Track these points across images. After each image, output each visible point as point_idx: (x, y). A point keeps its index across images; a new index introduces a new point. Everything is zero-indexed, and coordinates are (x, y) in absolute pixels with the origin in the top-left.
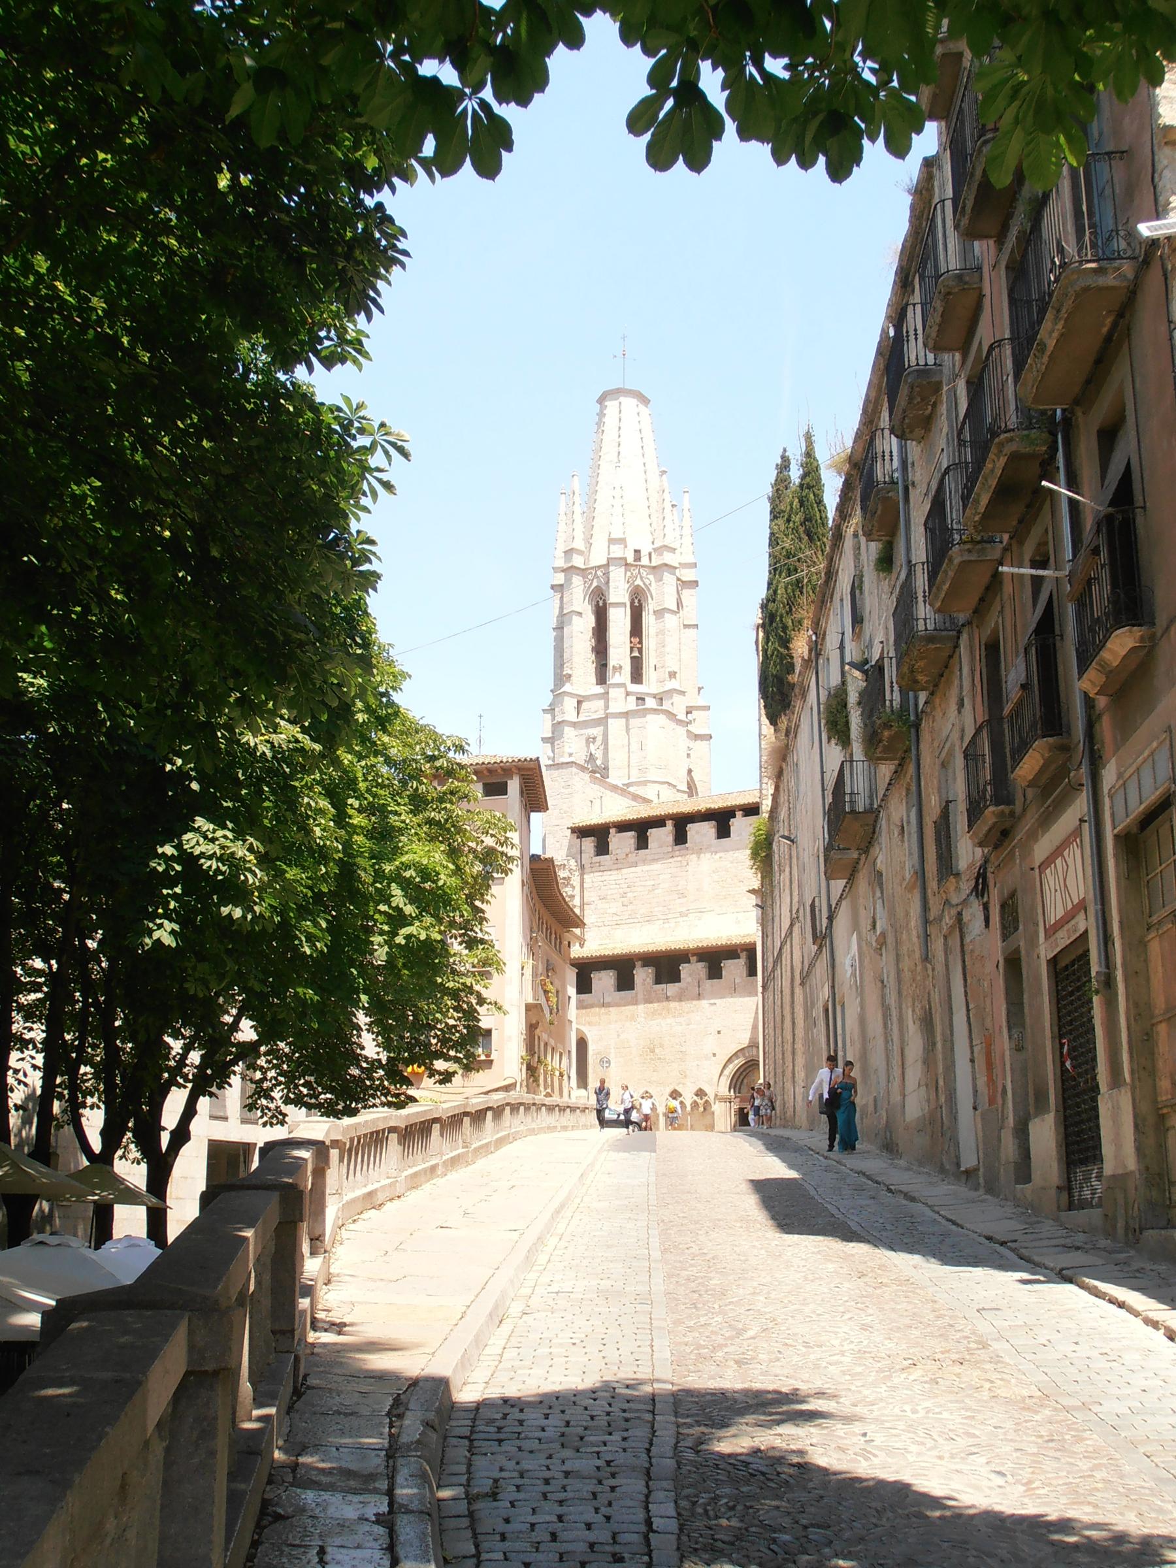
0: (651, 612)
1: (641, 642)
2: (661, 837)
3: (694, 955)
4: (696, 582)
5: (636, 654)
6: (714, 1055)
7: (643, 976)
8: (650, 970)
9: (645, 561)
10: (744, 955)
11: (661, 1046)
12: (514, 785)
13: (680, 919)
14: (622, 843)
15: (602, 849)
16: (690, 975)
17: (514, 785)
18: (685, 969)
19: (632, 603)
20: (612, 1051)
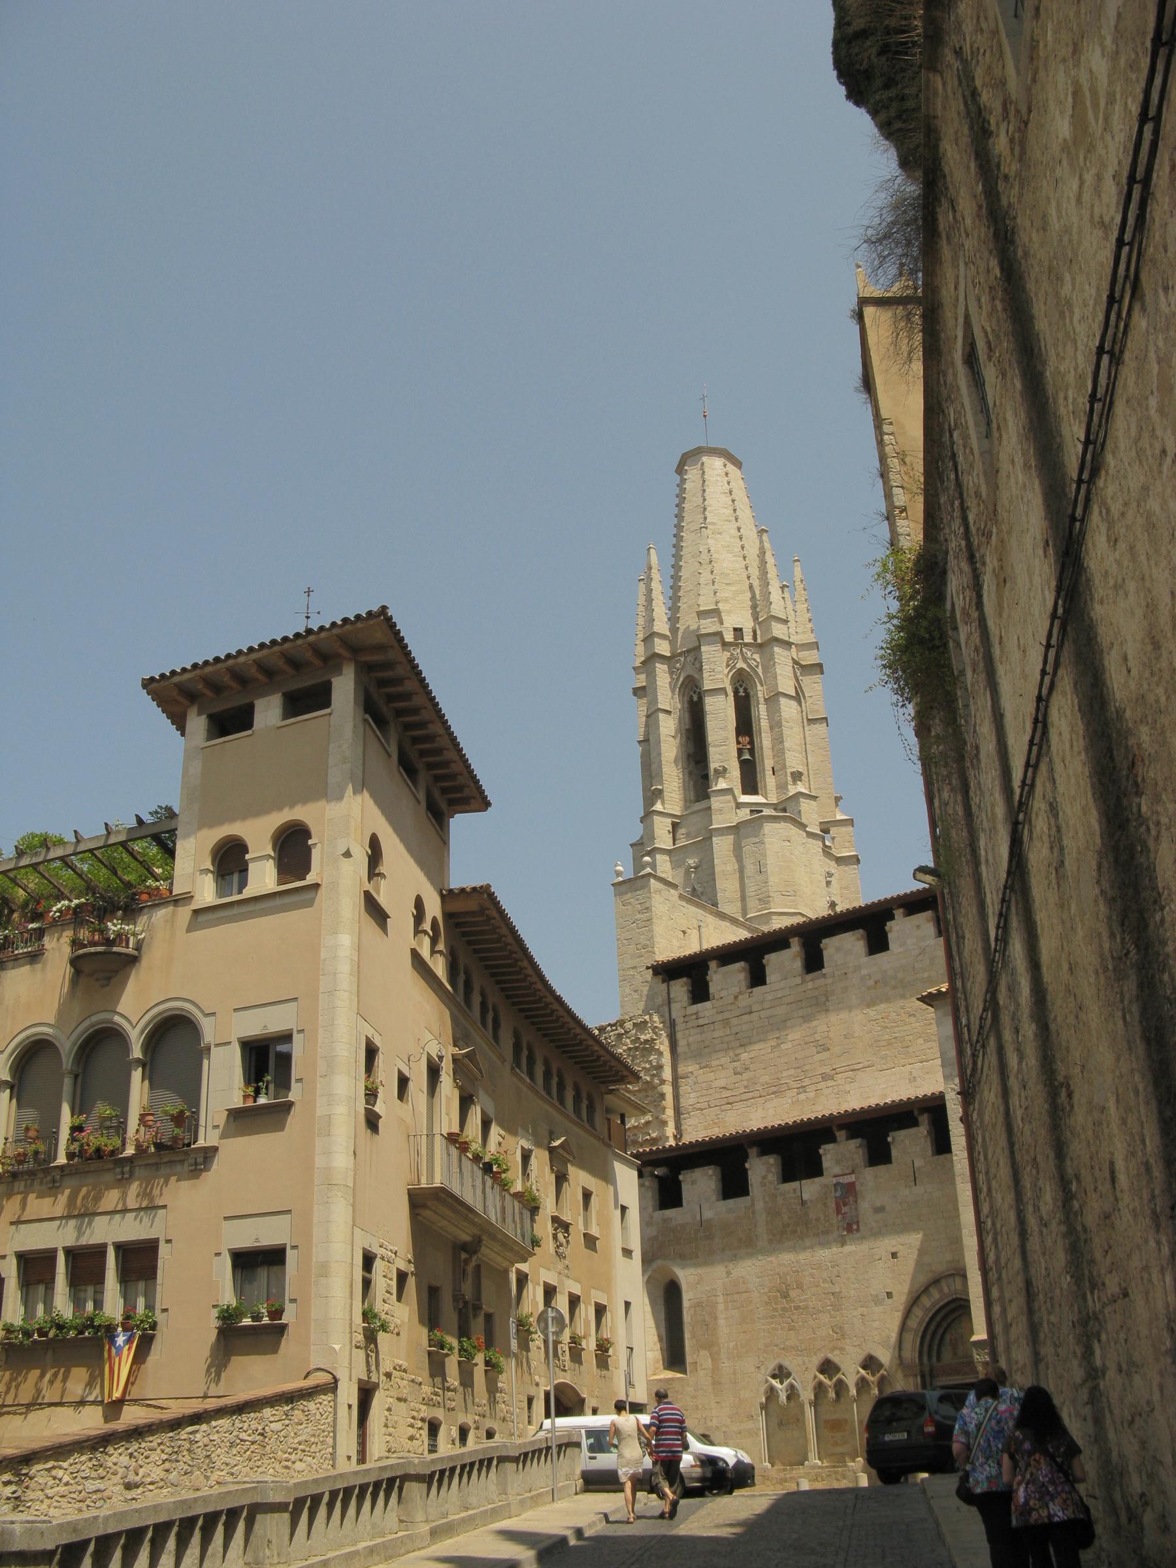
0: (762, 700)
1: (751, 742)
2: (784, 964)
3: (841, 1127)
4: (820, 666)
5: (747, 756)
6: (889, 1295)
7: (761, 1170)
8: (772, 1160)
9: (748, 639)
10: (924, 1119)
11: (800, 1286)
12: (344, 687)
13: (823, 1085)
14: (726, 981)
15: (700, 993)
16: (838, 1162)
17: (344, 687)
18: (829, 1154)
19: (736, 692)
20: (721, 1299)
